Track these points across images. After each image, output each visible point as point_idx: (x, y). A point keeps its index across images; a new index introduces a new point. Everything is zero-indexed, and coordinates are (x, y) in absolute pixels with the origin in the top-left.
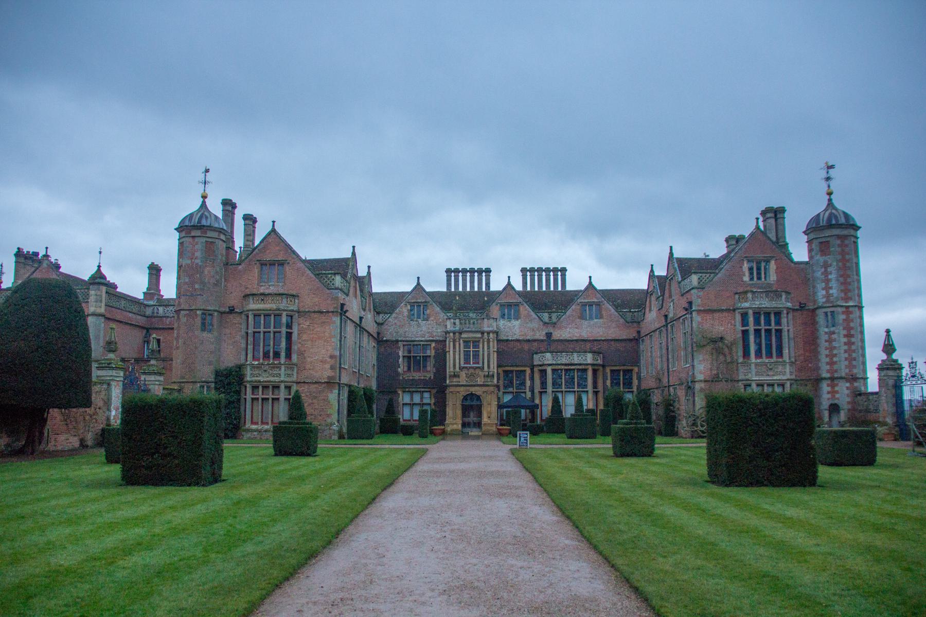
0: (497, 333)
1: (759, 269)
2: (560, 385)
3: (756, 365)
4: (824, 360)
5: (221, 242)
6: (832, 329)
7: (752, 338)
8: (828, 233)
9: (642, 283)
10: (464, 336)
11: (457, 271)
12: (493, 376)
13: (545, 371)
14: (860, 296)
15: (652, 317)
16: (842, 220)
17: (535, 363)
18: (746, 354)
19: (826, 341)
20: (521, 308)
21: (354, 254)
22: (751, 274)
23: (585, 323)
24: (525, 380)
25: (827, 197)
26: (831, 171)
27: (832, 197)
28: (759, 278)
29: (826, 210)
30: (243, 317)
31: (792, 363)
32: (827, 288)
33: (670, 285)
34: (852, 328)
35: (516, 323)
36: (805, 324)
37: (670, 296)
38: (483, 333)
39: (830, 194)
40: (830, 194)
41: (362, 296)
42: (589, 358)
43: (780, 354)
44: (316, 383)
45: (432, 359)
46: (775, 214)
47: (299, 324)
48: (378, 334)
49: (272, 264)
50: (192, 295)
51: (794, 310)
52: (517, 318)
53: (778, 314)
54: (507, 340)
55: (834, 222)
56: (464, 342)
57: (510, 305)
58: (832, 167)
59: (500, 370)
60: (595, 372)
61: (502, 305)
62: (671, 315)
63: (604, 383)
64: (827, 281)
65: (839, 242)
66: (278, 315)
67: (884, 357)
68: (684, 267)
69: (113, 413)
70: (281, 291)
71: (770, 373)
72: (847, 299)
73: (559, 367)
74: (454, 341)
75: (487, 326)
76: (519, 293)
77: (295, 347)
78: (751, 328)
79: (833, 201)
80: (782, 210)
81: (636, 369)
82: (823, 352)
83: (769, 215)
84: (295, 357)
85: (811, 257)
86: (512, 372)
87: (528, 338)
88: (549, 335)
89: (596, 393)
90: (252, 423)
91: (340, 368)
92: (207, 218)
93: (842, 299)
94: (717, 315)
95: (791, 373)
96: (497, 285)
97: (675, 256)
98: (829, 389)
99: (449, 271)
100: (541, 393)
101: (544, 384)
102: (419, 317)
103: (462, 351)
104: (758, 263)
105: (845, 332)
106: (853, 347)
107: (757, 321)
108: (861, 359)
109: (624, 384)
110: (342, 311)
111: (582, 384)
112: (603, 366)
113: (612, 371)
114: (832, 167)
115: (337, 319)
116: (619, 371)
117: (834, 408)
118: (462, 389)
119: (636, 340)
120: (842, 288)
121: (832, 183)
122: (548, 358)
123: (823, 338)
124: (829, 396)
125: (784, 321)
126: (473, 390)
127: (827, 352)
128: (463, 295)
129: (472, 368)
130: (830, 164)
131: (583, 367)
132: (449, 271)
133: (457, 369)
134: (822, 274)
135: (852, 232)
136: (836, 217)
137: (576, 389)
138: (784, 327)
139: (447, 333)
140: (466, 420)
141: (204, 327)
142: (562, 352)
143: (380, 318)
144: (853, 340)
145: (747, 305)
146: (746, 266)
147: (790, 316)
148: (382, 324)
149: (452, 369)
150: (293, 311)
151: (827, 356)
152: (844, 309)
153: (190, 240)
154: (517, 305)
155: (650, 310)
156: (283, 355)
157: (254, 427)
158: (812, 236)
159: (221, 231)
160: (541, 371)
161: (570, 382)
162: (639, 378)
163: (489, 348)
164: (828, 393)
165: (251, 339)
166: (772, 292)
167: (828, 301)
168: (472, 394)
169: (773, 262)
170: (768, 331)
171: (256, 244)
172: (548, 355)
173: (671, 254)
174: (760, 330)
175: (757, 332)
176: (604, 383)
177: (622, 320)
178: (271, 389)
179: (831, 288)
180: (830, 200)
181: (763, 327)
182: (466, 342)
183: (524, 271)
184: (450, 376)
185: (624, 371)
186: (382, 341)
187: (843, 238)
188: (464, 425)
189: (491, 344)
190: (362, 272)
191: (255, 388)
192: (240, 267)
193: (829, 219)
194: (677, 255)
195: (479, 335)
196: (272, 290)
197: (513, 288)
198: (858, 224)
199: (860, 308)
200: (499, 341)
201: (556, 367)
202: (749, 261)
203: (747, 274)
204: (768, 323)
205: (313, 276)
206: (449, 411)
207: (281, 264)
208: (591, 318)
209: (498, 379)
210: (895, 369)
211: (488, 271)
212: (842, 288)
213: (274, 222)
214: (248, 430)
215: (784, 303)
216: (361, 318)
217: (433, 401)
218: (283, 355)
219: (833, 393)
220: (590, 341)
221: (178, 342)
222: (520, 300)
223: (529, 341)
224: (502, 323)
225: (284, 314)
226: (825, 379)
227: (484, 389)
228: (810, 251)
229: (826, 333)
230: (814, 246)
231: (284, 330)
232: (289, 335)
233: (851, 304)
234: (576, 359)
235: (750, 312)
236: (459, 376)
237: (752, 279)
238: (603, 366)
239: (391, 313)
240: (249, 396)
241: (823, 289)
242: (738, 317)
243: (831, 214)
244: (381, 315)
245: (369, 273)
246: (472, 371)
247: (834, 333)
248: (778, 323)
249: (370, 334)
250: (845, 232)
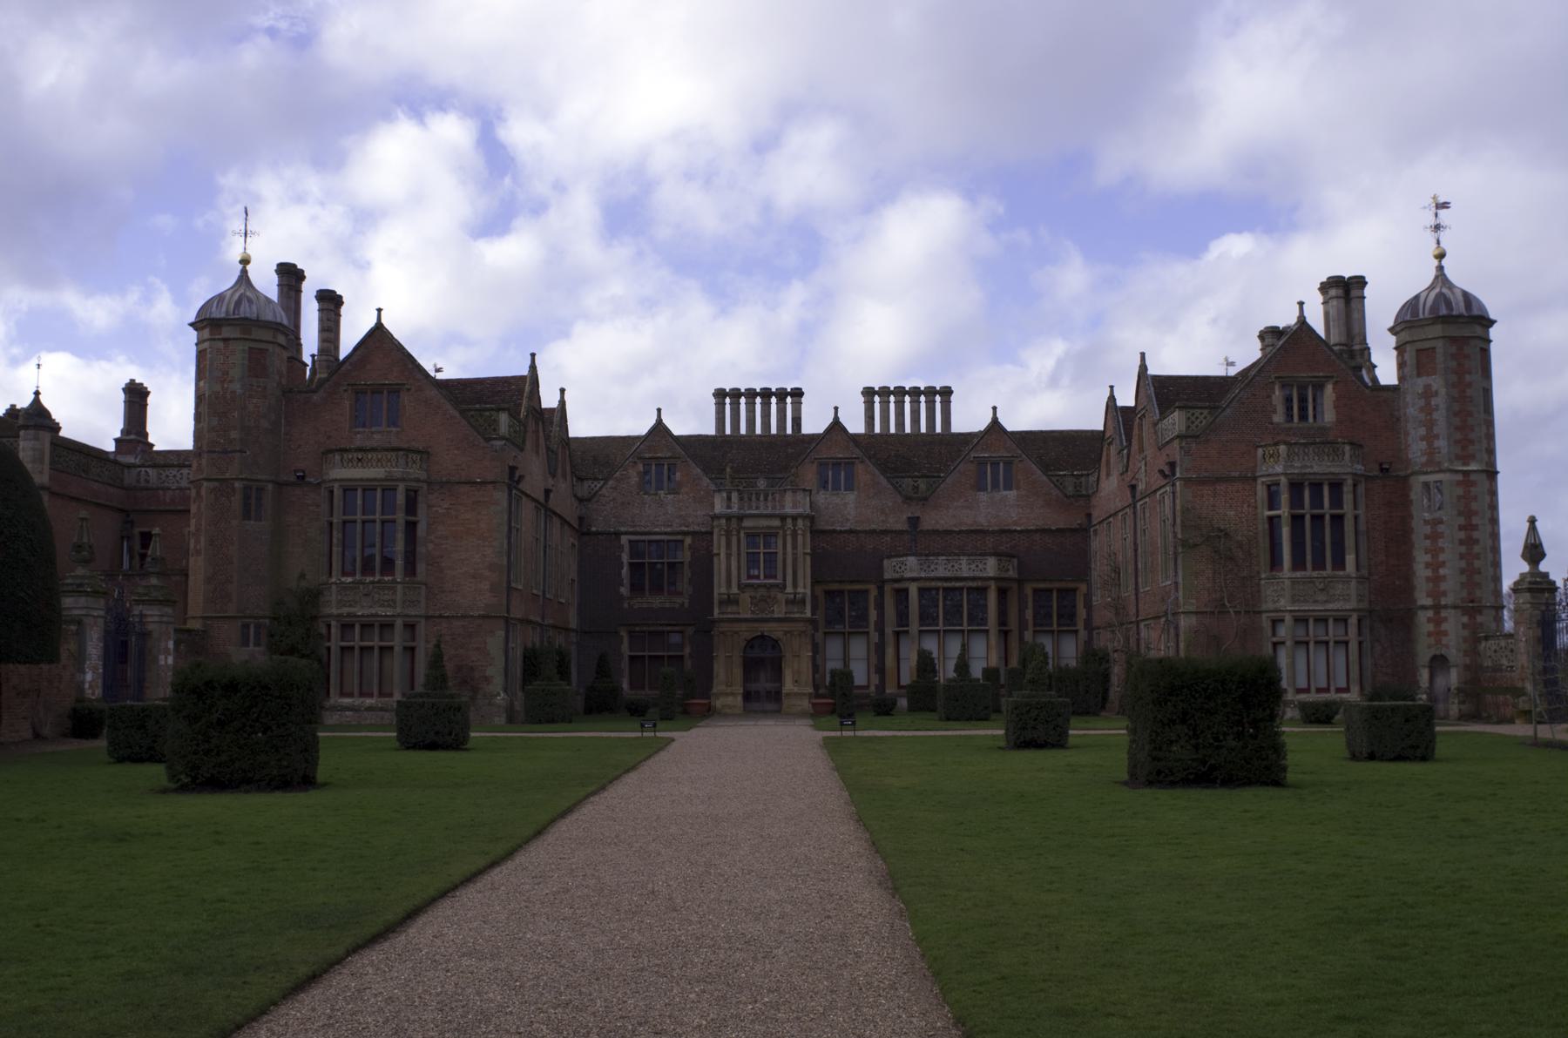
0: (812, 519)
1: (1303, 400)
2: (935, 621)
3: (1294, 581)
4: (1421, 572)
5: (278, 349)
6: (1438, 514)
7: (1286, 532)
9: (1094, 421)
10: (747, 523)
11: (736, 394)
12: (803, 602)
13: (906, 591)
14: (1491, 452)
15: (1110, 488)
16: (1459, 308)
17: (887, 576)
18: (1275, 563)
19: (1427, 537)
20: (859, 468)
21: (533, 367)
22: (1289, 409)
23: (983, 496)
24: (866, 609)
25: (1436, 262)
26: (1442, 212)
27: (1444, 262)
28: (1303, 416)
29: (1431, 288)
30: (324, 492)
31: (1361, 579)
33: (1141, 426)
34: (1476, 513)
35: (851, 497)
37: (1141, 450)
38: (783, 518)
41: (548, 448)
42: (991, 567)
43: (1339, 563)
44: (463, 617)
45: (686, 567)
46: (1345, 292)
47: (429, 507)
48: (581, 519)
49: (377, 390)
50: (225, 452)
51: (1367, 478)
52: (849, 488)
53: (1336, 486)
54: (834, 531)
55: (1444, 311)
56: (748, 535)
57: (837, 464)
58: (1445, 205)
59: (819, 590)
60: (1002, 593)
61: (823, 465)
62: (1141, 487)
63: (1021, 612)
64: (1429, 425)
65: (1453, 349)
66: (389, 490)
67: (1525, 567)
68: (1165, 392)
69: (89, 677)
70: (396, 443)
71: (1321, 597)
72: (1466, 459)
73: (933, 584)
74: (728, 534)
75: (792, 504)
76: (855, 438)
77: (421, 550)
78: (1284, 511)
79: (1446, 271)
80: (1360, 282)
81: (1083, 588)
82: (1421, 558)
83: (1333, 292)
84: (421, 568)
85: (1401, 378)
86: (841, 592)
87: (873, 527)
88: (914, 522)
89: (1005, 634)
90: (343, 694)
91: (509, 589)
92: (250, 301)
93: (1458, 457)
94: (1221, 487)
96: (814, 423)
97: (1152, 371)
98: (1431, 627)
99: (720, 394)
100: (897, 634)
101: (903, 618)
102: (660, 488)
103: (744, 556)
104: (1302, 389)
105: (1462, 521)
106: (1477, 549)
107: (1296, 501)
108: (1491, 570)
109: (1060, 616)
110: (513, 478)
111: (977, 617)
112: (1020, 582)
113: (1035, 591)
114: (1445, 205)
115: (501, 496)
116: (1051, 591)
117: (1439, 663)
118: (744, 626)
119: (1083, 532)
120: (1458, 436)
121: (1445, 236)
122: (911, 566)
124: (1432, 640)
125: (1348, 498)
126: (766, 628)
127: (1428, 558)
128: (750, 442)
129: (765, 586)
130: (1441, 200)
131: (980, 584)
132: (720, 394)
133: (735, 590)
134: (1421, 410)
135: (1479, 330)
136: (1448, 303)
137: (965, 627)
138: (1347, 508)
139: (715, 517)
140: (753, 687)
141: (247, 515)
142: (939, 555)
143: (584, 489)
144: (1476, 535)
145: (1279, 469)
147: (1361, 489)
148: (589, 500)
149: (723, 590)
150: (418, 480)
151: (1428, 565)
152: (1460, 477)
153: (221, 345)
154: (850, 464)
155: (1108, 475)
156: (399, 563)
157: (347, 701)
158: (1405, 336)
159: (276, 327)
160: (898, 591)
161: (953, 614)
162: (1088, 606)
163: (795, 547)
164: (1430, 634)
165: (337, 535)
166: (1323, 442)
167: (1430, 462)
168: (762, 636)
169: (1329, 388)
170: (1318, 518)
171: (342, 356)
172: (912, 560)
173: (1143, 368)
174: (1302, 517)
175: (1297, 520)
176: (1021, 612)
177: (1055, 492)
178: (377, 630)
179: (1437, 437)
180: (1440, 268)
181: (1307, 510)
182: (752, 536)
183: (869, 393)
184: (721, 603)
185: (1059, 590)
186: (589, 533)
187: (1465, 340)
188: (748, 696)
189: (800, 538)
190: (549, 400)
191: (346, 627)
192: (315, 397)
194: (1152, 371)
195: (777, 523)
196: (377, 440)
197: (844, 429)
198: (1492, 316)
199: (1492, 474)
200: (816, 533)
201: (928, 584)
202: (1283, 386)
203: (1281, 409)
204: (1317, 501)
205: (457, 414)
206: (719, 669)
207: (395, 390)
208: (995, 486)
209: (814, 610)
210: (1542, 591)
211: (797, 394)
212: (1458, 436)
213: (379, 310)
214: (335, 708)
216: (547, 492)
217: (687, 650)
218: (399, 563)
219: (1439, 634)
220: (993, 532)
221: (197, 542)
222: (857, 452)
223: (873, 532)
224: (822, 498)
225: (401, 488)
226: (1424, 608)
227: (786, 627)
228: (1401, 365)
229: (1426, 522)
230: (1407, 356)
231: (401, 517)
232: (411, 527)
233: (1473, 467)
234: (964, 567)
236: (736, 602)
237: (1289, 417)
238: (1020, 582)
239: (606, 480)
240: (335, 643)
241: (1422, 439)
242: (1261, 492)
243: (1441, 294)
244: (586, 484)
245: (562, 403)
246: (762, 591)
247: (1441, 522)
248: (1337, 501)
249: (564, 521)
250: (1466, 332)
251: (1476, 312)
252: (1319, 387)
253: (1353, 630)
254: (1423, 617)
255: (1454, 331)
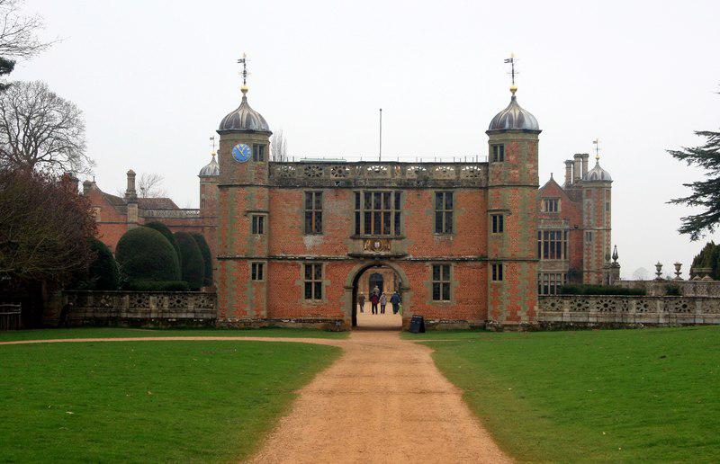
1: (551, 204)
3: (544, 263)
7: (542, 247)
8: (591, 185)
14: (609, 223)
28: (551, 210)
32: (589, 218)
36: (578, 238)
39: (598, 159)
40: (598, 159)
43: (559, 257)
78: (542, 241)
95: (566, 268)
107: (546, 237)
123: (585, 247)
146: (543, 203)
147: (568, 233)
166: (555, 218)
181: (549, 241)
193: (592, 177)
199: (609, 230)
203: (544, 207)
204: (553, 238)
215: (563, 226)
235: (542, 232)
251: (605, 179)
252: (556, 200)
253: (563, 278)
254: (585, 274)
255: (595, 185)
